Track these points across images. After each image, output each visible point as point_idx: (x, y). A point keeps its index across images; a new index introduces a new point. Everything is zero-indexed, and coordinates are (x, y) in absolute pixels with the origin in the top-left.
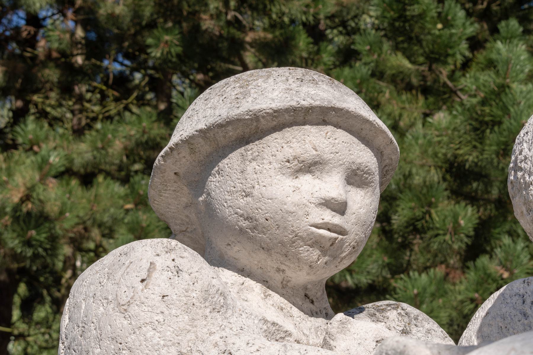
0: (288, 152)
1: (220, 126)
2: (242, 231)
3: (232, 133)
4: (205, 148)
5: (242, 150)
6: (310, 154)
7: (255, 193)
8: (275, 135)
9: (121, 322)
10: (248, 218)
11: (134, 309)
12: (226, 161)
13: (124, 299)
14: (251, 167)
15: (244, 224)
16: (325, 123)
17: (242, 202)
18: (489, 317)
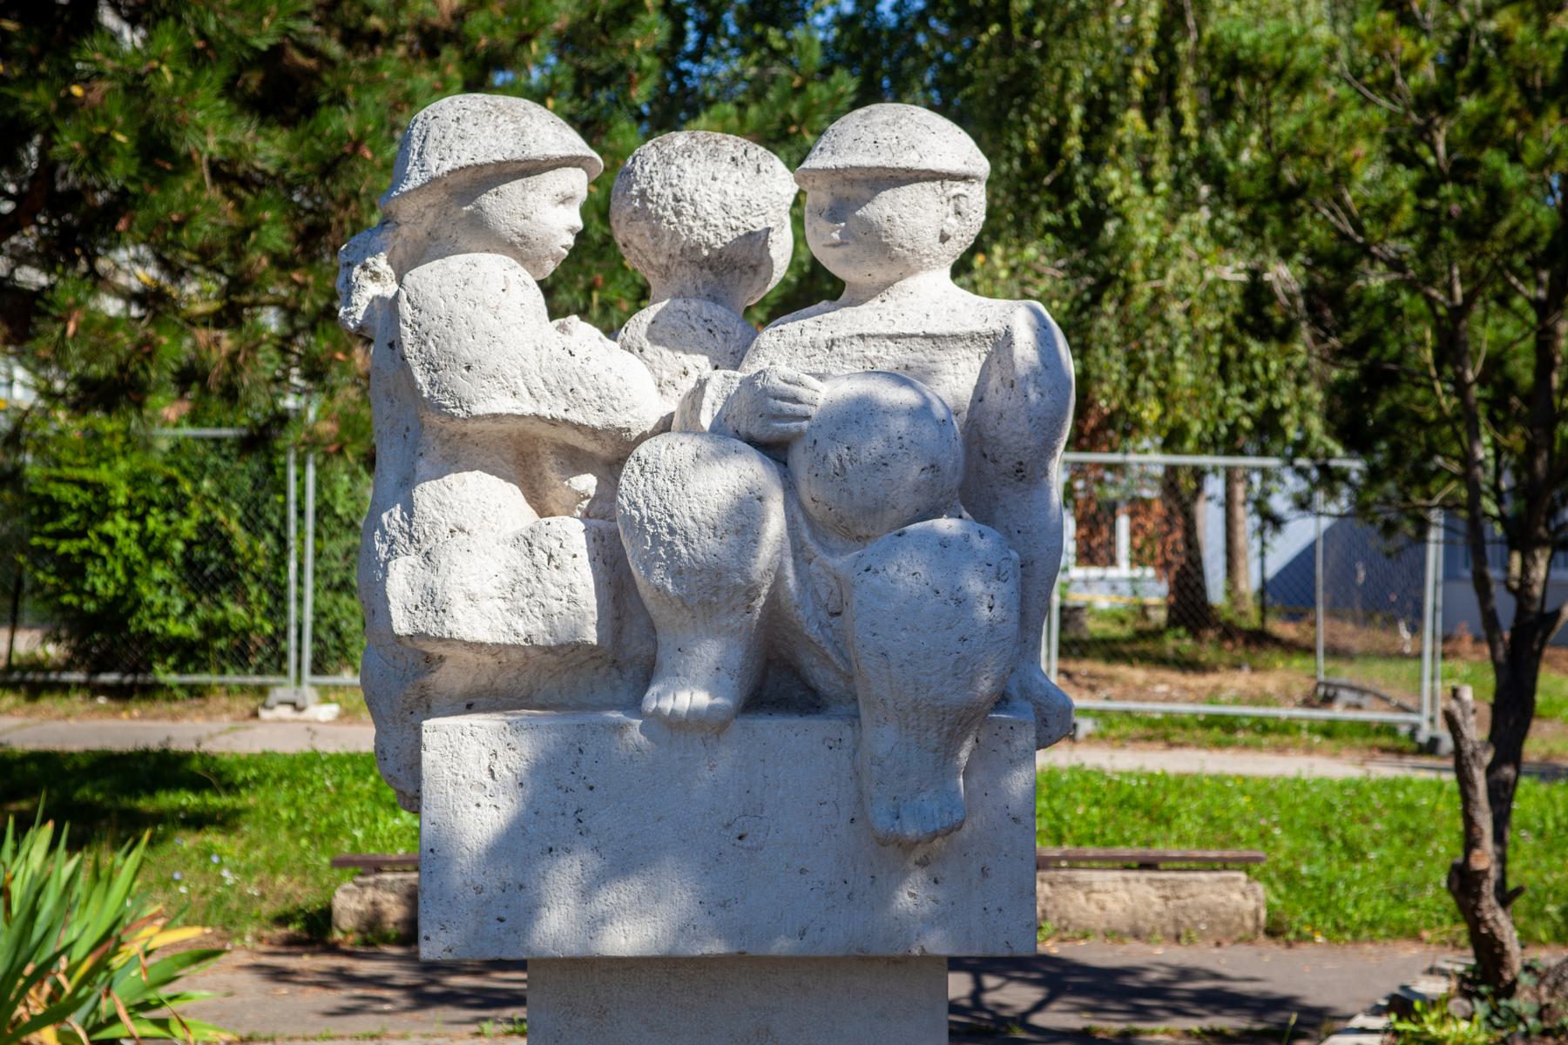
0: (558, 188)
1: (519, 162)
2: (512, 244)
3: (522, 166)
4: (489, 171)
5: (523, 180)
6: (568, 192)
7: (533, 217)
8: (551, 173)
9: (492, 320)
10: (523, 236)
11: (501, 312)
12: (507, 186)
13: (493, 305)
14: (531, 196)
15: (517, 239)
16: (578, 166)
17: (520, 223)
18: (658, 326)
